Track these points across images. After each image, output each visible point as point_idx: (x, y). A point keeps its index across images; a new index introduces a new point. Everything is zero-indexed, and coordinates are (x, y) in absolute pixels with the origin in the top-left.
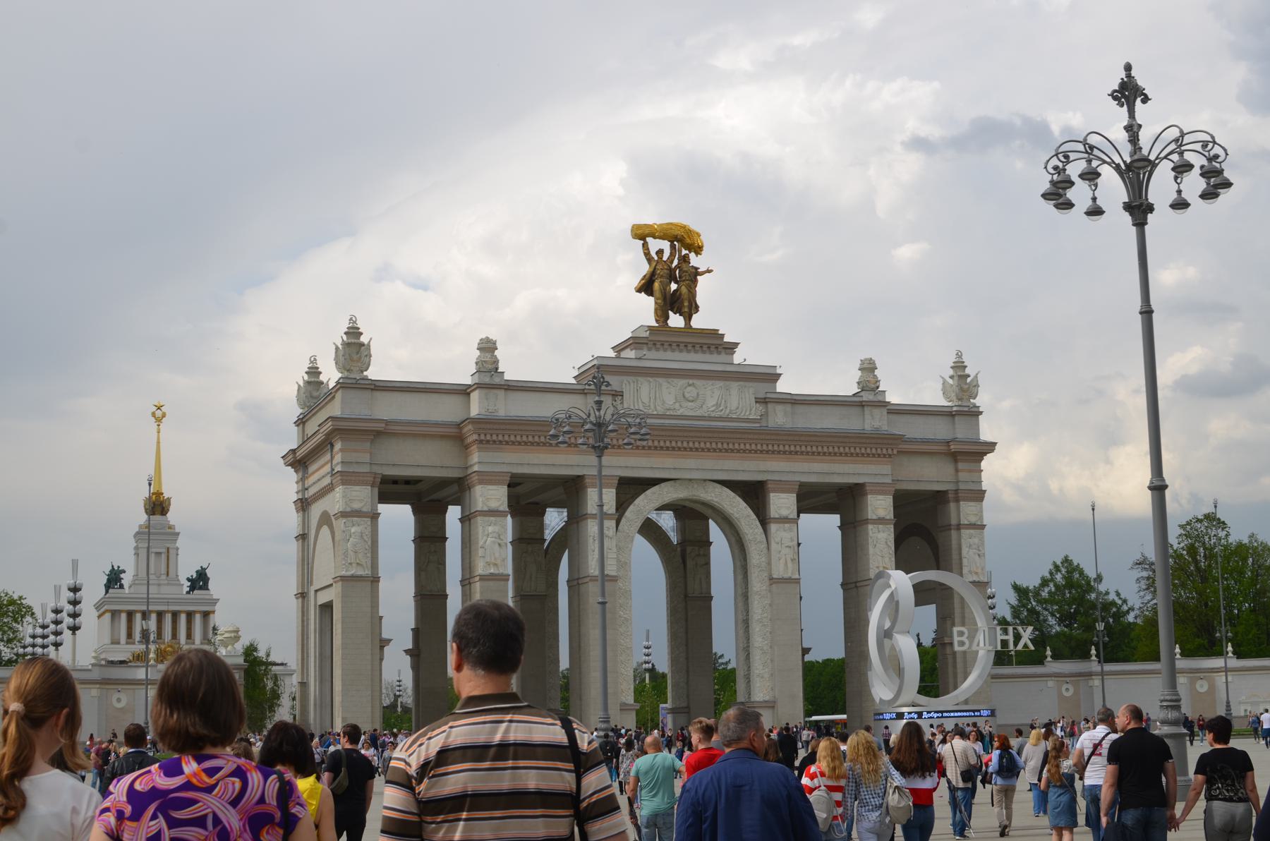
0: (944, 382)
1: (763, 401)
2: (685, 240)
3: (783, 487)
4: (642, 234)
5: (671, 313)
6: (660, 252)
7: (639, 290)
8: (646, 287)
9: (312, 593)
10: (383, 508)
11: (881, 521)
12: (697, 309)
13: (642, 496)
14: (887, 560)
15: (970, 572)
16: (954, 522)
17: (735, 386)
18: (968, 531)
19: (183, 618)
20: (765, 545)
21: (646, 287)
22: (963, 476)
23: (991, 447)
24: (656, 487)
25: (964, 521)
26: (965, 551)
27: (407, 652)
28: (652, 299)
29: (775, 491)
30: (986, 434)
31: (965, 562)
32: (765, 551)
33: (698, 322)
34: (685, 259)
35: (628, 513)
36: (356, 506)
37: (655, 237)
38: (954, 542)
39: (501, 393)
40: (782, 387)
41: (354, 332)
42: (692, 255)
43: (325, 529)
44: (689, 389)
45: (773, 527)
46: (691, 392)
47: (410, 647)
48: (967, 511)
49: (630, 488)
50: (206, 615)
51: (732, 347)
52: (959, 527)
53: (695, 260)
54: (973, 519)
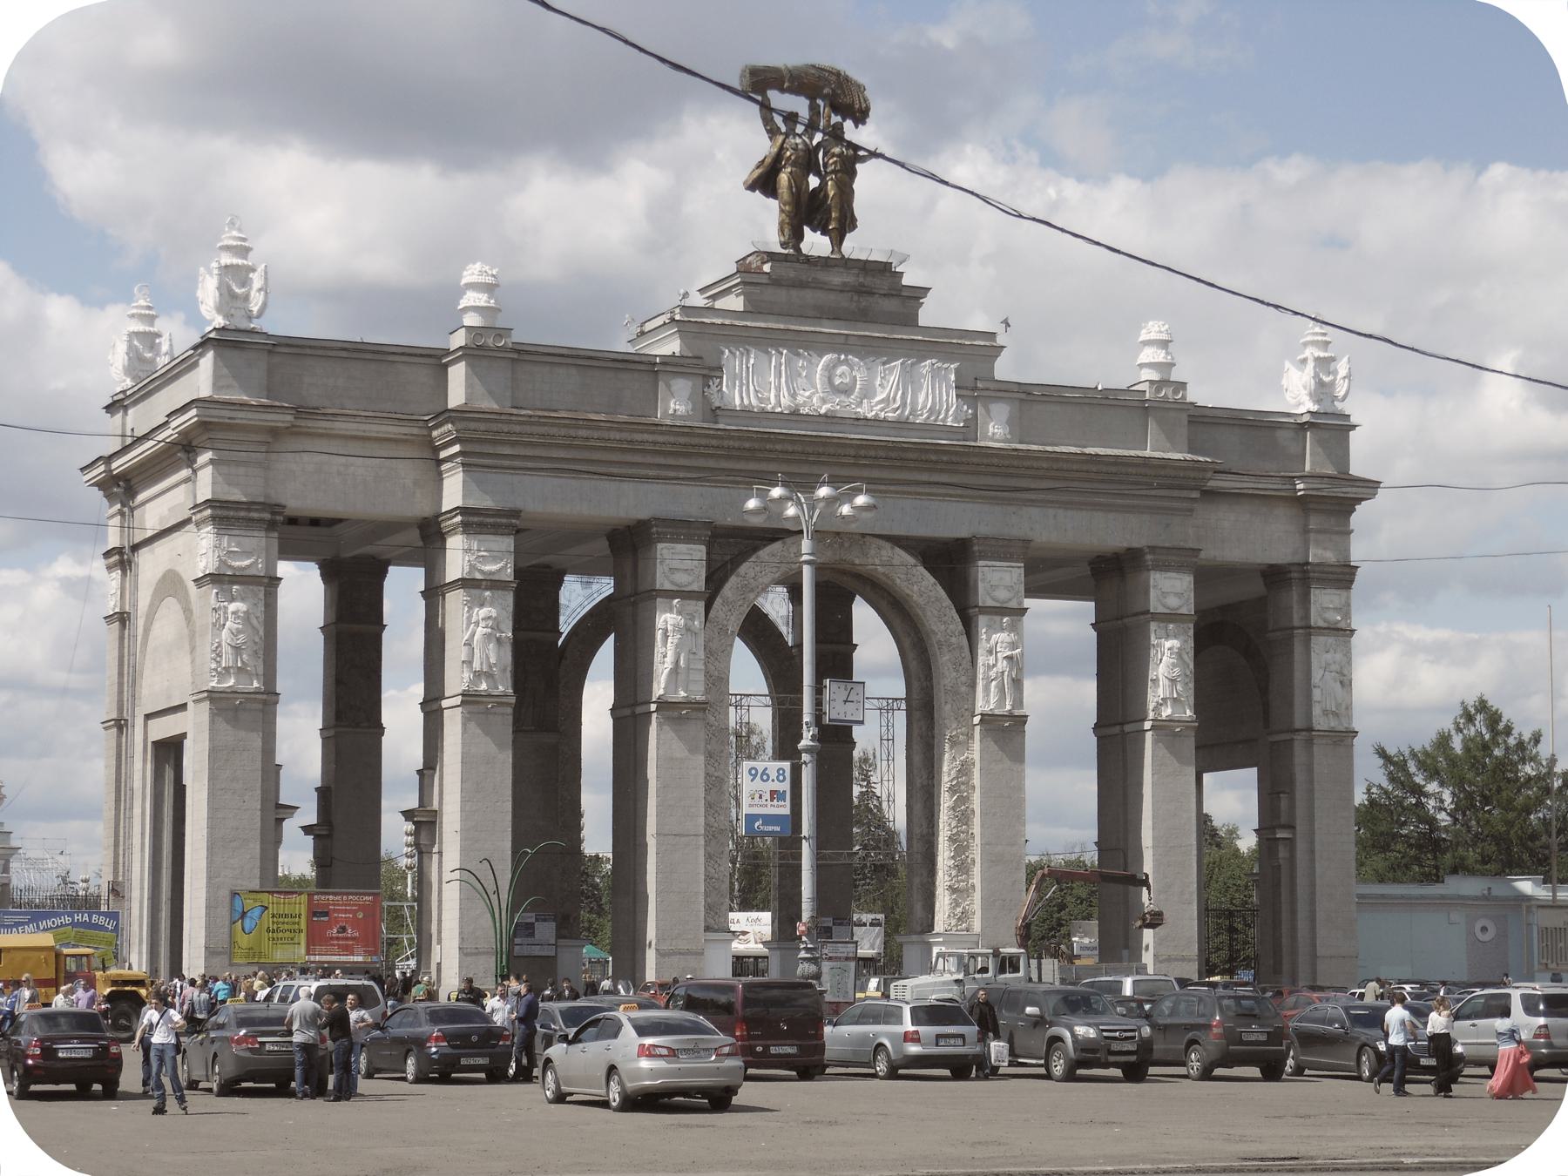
2: (838, 97)
3: (1003, 549)
5: (806, 229)
7: (752, 187)
8: (765, 182)
9: (139, 721)
10: (285, 568)
12: (853, 226)
15: (1325, 712)
21: (765, 182)
23: (1370, 487)
25: (1315, 620)
28: (774, 204)
31: (1316, 694)
32: (966, 663)
33: (852, 246)
34: (836, 134)
37: (782, 90)
40: (1004, 369)
42: (848, 125)
43: (171, 608)
45: (983, 621)
48: (1323, 601)
49: (732, 547)
52: (1309, 629)
53: (851, 132)
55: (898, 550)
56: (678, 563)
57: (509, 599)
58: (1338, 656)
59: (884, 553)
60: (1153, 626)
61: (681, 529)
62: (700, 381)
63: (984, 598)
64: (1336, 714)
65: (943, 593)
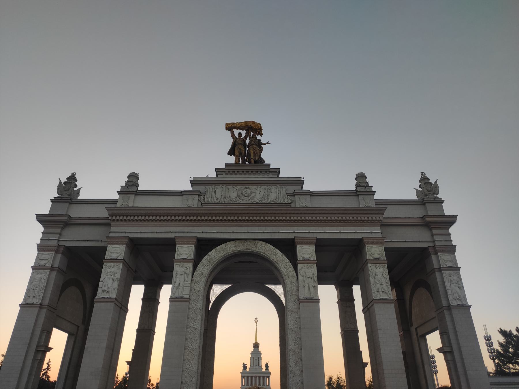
0: (417, 190)
1: (293, 195)
2: (254, 129)
3: (306, 241)
4: (230, 127)
6: (240, 134)
11: (376, 261)
13: (214, 250)
14: (384, 286)
15: (455, 299)
16: (436, 266)
17: (273, 189)
18: (447, 272)
19: (262, 378)
20: (295, 278)
22: (436, 238)
24: (223, 246)
25: (443, 265)
26: (448, 285)
27: (128, 363)
29: (300, 244)
30: (448, 210)
31: (449, 292)
32: (295, 282)
35: (203, 261)
36: (43, 263)
38: (439, 280)
39: (132, 196)
41: (72, 179)
44: (245, 190)
46: (249, 191)
47: (130, 360)
48: (444, 258)
50: (268, 377)
51: (277, 171)
52: (440, 270)
53: (259, 137)
54: (450, 264)
55: (268, 244)
56: (185, 251)
57: (121, 265)
58: (455, 278)
59: (263, 245)
60: (369, 265)
61: (186, 241)
62: (197, 196)
63: (299, 257)
64: (460, 300)
65: (284, 257)
